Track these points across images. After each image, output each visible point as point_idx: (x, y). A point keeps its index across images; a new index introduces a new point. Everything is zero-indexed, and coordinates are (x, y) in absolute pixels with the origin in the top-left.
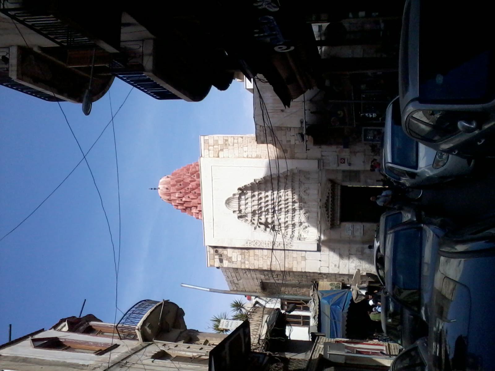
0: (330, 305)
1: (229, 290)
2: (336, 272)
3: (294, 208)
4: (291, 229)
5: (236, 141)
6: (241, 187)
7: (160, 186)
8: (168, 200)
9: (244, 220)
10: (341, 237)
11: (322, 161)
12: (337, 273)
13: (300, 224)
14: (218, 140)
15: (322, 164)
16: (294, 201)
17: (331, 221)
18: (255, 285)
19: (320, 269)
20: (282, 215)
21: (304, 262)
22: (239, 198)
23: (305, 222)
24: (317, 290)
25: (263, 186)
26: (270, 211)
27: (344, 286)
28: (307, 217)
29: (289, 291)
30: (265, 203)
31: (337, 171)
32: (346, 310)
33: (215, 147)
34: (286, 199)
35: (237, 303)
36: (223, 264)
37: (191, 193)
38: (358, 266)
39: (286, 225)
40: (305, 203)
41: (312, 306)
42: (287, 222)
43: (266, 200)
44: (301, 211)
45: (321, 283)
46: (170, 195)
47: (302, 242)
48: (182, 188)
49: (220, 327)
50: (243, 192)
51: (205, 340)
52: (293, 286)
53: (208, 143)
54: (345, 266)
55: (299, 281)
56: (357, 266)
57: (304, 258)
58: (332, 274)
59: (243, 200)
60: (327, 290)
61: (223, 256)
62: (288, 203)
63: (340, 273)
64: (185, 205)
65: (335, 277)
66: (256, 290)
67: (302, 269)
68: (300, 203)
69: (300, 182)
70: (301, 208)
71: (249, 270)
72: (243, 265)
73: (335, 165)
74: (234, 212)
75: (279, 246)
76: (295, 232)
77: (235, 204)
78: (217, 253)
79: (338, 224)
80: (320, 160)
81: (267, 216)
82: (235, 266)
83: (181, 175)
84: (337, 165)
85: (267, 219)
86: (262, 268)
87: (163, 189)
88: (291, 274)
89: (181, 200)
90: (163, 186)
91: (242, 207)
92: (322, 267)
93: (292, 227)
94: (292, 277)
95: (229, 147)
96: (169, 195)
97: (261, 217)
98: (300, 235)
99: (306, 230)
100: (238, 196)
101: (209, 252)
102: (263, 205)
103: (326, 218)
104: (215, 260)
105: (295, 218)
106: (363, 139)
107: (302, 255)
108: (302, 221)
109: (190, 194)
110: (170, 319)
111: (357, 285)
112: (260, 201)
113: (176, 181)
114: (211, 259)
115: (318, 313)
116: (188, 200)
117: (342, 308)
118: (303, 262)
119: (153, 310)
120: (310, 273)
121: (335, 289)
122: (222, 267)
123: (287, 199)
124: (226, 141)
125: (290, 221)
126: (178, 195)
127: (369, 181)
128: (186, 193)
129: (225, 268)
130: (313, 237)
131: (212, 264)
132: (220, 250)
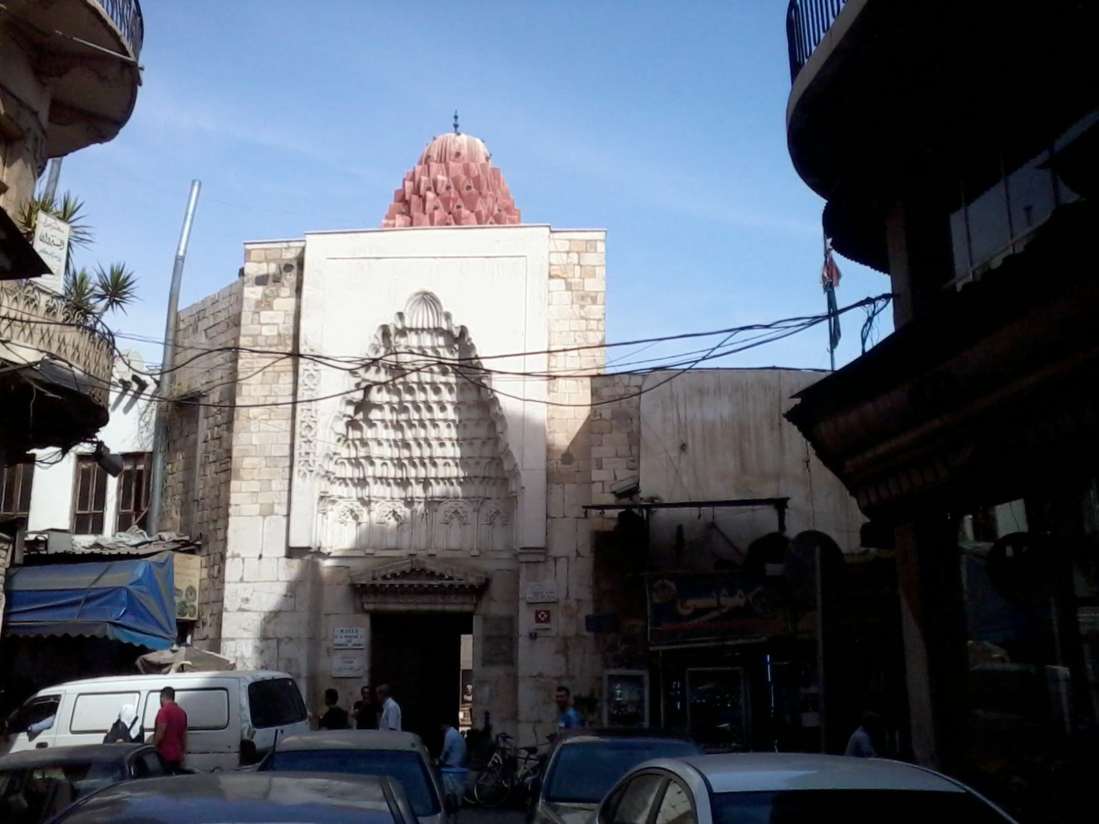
0: (130, 588)
1: (180, 308)
2: (227, 603)
3: (411, 484)
4: (351, 476)
5: (593, 324)
6: (470, 335)
7: (463, 138)
8: (429, 157)
9: (376, 342)
11: (542, 558)
12: (225, 606)
13: (366, 499)
14: (595, 277)
16: (431, 484)
17: (373, 585)
18: (192, 379)
19: (233, 557)
20: (392, 452)
21: (258, 512)
22: (438, 331)
23: (372, 513)
24: (174, 550)
25: (472, 396)
26: (403, 416)
27: (185, 628)
28: (386, 519)
29: (174, 475)
30: (426, 402)
31: (514, 598)
32: (113, 634)
33: (577, 268)
34: (436, 460)
35: (125, 287)
36: (252, 286)
37: (446, 214)
38: (245, 664)
39: (362, 461)
40: (425, 515)
41: (131, 539)
42: (372, 464)
43: (431, 404)
44: (403, 501)
45: (196, 561)
46: (441, 162)
47: (316, 505)
48: (460, 192)
49: (42, 216)
50: (456, 340)
51: (8, 184)
52: (188, 484)
53: (587, 252)
54: (244, 629)
55: (202, 499)
56: (245, 661)
57: (267, 512)
58: (220, 590)
59: (432, 340)
60: (176, 577)
61: (275, 286)
62: (424, 465)
63: (224, 614)
64: (415, 198)
65: (213, 602)
66: (177, 383)
67: (236, 505)
68: (423, 500)
69: (481, 500)
70: (409, 502)
71: (233, 357)
72: (248, 340)
73: (531, 596)
74: (401, 315)
75: (305, 439)
76: (343, 485)
77: (421, 317)
78: (284, 269)
79: (366, 606)
80: (544, 554)
81: (387, 407)
82: (246, 318)
83: (494, 191)
84: (531, 601)
85: (380, 407)
86: (241, 394)
87: (457, 144)
88: (223, 476)
89: (429, 189)
90: (465, 144)
91: (413, 340)
92: (241, 561)
93: (358, 479)
94: (213, 479)
95: (576, 307)
96: (442, 159)
97: (384, 391)
98: (334, 502)
99: (347, 517)
100: (444, 326)
101: (289, 248)
102: (420, 397)
103: (383, 573)
104: (264, 265)
105: (382, 487)
106: (613, 672)
107: (276, 506)
108: (373, 504)
109: (445, 210)
110: (80, 86)
111: (189, 663)
112: (431, 388)
113: (479, 176)
114: (268, 252)
115: (106, 552)
116: (429, 206)
117: (118, 622)
118: (256, 509)
119: (104, 22)
120: (226, 528)
121: (177, 600)
122: (244, 283)
123: (435, 464)
124: (592, 299)
125: (374, 472)
126: (443, 182)
127: (486, 690)
128: (446, 202)
129: (241, 292)
130: (329, 538)
131: (253, 256)
132: (291, 277)
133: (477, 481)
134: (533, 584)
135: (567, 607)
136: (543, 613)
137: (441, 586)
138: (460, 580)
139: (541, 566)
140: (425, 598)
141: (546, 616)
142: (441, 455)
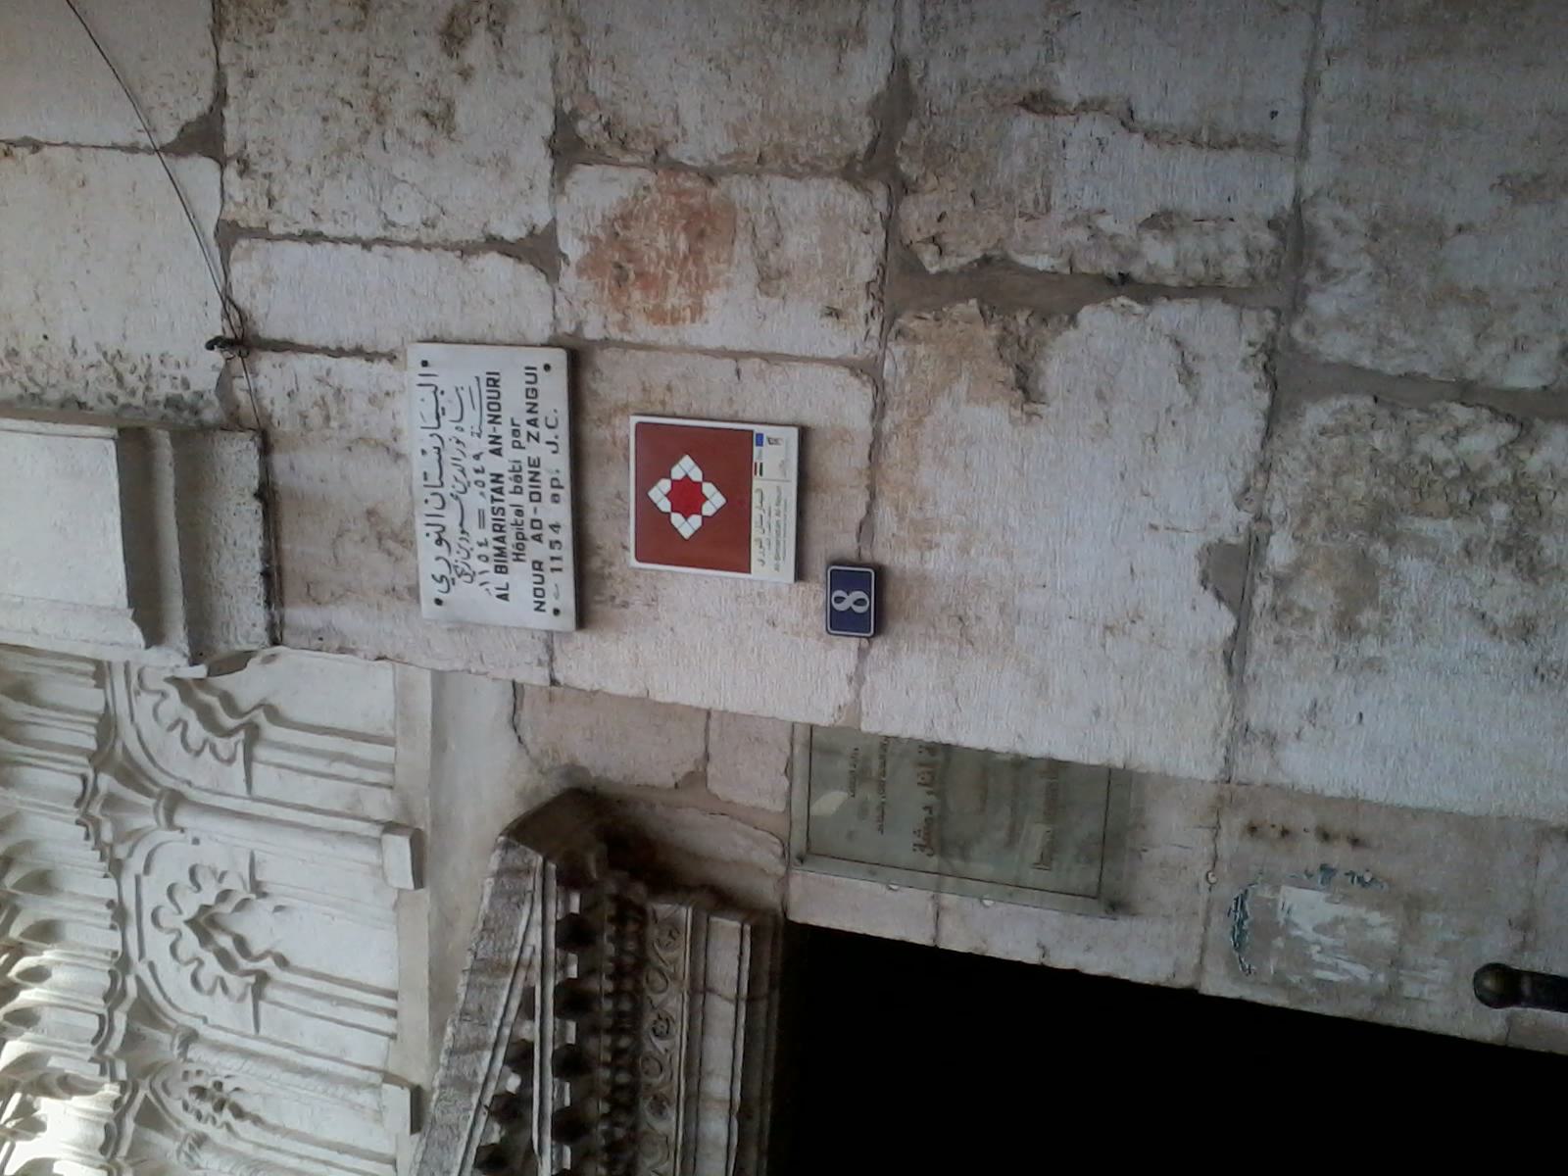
11: (238, 459)
15: (239, 529)
69: (106, 782)
73: (520, 578)
84: (562, 587)
134: (428, 560)
135: (618, 264)
136: (660, 493)
137: (569, 1127)
138: (527, 1009)
139: (305, 467)
141: (686, 468)
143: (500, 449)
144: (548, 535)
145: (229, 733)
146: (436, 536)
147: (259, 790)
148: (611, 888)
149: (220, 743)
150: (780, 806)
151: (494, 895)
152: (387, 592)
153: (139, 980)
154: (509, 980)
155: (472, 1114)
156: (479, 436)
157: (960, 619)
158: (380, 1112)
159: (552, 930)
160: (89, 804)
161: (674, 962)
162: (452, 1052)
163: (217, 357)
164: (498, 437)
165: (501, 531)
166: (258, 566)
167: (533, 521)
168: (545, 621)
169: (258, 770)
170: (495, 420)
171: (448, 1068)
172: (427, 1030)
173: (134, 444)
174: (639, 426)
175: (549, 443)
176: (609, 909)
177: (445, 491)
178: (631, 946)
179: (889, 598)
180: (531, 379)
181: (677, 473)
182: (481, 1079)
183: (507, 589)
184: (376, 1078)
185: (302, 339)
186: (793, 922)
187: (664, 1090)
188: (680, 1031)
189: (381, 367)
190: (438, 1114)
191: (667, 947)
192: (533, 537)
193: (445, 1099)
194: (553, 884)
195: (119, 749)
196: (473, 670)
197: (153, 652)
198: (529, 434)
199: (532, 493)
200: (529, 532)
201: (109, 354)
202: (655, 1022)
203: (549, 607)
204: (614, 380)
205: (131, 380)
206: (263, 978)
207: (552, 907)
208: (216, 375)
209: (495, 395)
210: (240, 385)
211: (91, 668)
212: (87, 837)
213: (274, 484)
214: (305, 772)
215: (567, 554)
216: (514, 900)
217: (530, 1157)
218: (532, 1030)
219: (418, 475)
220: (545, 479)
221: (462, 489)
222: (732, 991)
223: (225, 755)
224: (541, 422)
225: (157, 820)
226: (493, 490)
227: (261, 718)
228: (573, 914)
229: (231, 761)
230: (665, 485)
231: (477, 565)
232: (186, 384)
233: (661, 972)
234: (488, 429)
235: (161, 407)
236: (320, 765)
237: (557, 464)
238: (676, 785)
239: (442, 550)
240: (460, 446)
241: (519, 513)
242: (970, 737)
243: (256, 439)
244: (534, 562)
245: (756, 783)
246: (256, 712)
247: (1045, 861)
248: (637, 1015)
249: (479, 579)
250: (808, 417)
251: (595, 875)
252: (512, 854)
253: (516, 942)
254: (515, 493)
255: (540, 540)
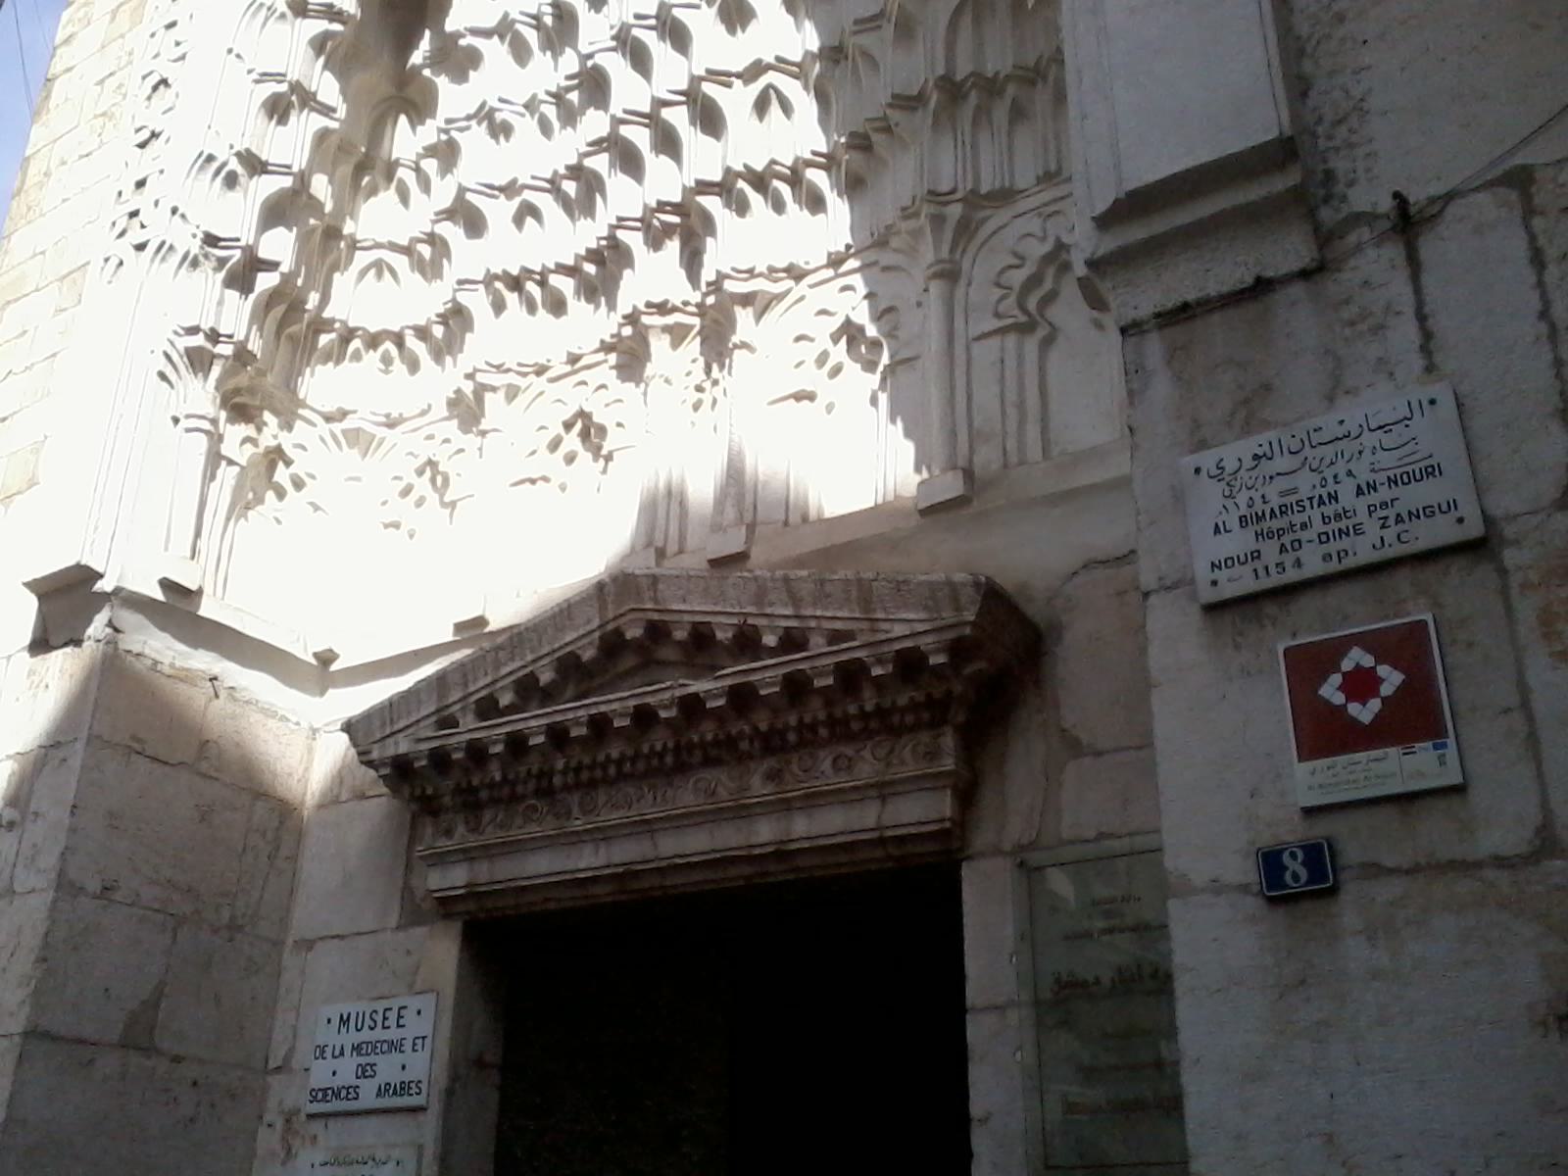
10: (308, 945)
11: (1289, 250)
15: (1224, 269)
16: (708, 223)
17: (440, 759)
62: (668, 142)
68: (696, 321)
69: (955, 211)
73: (1239, 542)
76: (399, 367)
84: (1240, 582)
133: (923, 119)
134: (1235, 452)
136: (1357, 658)
137: (742, 697)
138: (836, 637)
139: (1296, 316)
140: (686, 796)
142: (739, 68)
143: (1363, 494)
144: (1289, 559)
145: (1022, 306)
146: (1261, 454)
147: (976, 348)
148: (958, 688)
149: (1012, 300)
150: (1066, 833)
151: (930, 583)
152: (1195, 421)
153: (788, 291)
154: (857, 615)
155: (737, 610)
156: (1373, 471)
157: (1303, 982)
158: (720, 529)
159: (909, 644)
160: (930, 201)
161: (903, 763)
162: (786, 580)
163: (1386, 204)
164: (1375, 490)
165: (1281, 513)
166: (1191, 296)
167: (1299, 541)
168: (1202, 573)
169: (994, 342)
170: (1392, 482)
171: (773, 579)
172: (798, 552)
173: (1282, 152)
174: (1423, 624)
175: (1382, 538)
176: (938, 692)
177: (1307, 451)
178: (909, 719)
179: (1307, 905)
180: (1444, 508)
181: (1383, 670)
182: (768, 611)
183: (1226, 531)
184: (748, 517)
185: (1428, 280)
186: (961, 866)
187: (787, 777)
188: (843, 781)
189: (1418, 362)
190: (731, 581)
191: (914, 751)
192: (1283, 545)
193: (745, 584)
194: (950, 635)
195: (988, 212)
196: (1140, 518)
197: (1089, 225)
198: (1386, 518)
199: (1326, 534)
200: (1287, 539)
201: (1364, 104)
202: (846, 756)
203: (1217, 574)
204: (1463, 590)
205: (1343, 130)
206: (811, 397)
207: (929, 639)
208: (1368, 209)
209: (1418, 477)
210: (1364, 233)
211: (1053, 167)
212: (904, 209)
213: (1274, 290)
214: (1002, 379)
215: (1275, 580)
216: (930, 603)
217: (710, 670)
218: (818, 646)
219: (1318, 422)
220: (1345, 543)
221: (1313, 467)
222: (887, 820)
223: (1001, 308)
224: (1401, 527)
225: (931, 265)
226: (1320, 496)
227: (1042, 332)
228: (928, 659)
229: (997, 315)
230: (1368, 661)
231: (1242, 499)
232: (1351, 184)
233: (891, 751)
234: (1382, 477)
235: (1322, 167)
236: (1011, 396)
237: (1363, 552)
238: (1064, 730)
239: (1248, 462)
240: (1357, 455)
241: (1304, 526)
242: (1185, 1011)
243: (1314, 264)
244: (1259, 551)
245: (1085, 805)
246: (1046, 325)
247: (1070, 1108)
248: (850, 737)
249: (1229, 503)
250: (1478, 796)
251: (968, 670)
252: (970, 591)
253: (893, 614)
254: (1323, 517)
255: (1281, 552)
